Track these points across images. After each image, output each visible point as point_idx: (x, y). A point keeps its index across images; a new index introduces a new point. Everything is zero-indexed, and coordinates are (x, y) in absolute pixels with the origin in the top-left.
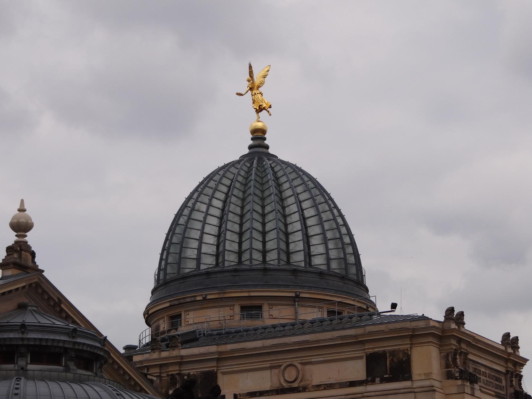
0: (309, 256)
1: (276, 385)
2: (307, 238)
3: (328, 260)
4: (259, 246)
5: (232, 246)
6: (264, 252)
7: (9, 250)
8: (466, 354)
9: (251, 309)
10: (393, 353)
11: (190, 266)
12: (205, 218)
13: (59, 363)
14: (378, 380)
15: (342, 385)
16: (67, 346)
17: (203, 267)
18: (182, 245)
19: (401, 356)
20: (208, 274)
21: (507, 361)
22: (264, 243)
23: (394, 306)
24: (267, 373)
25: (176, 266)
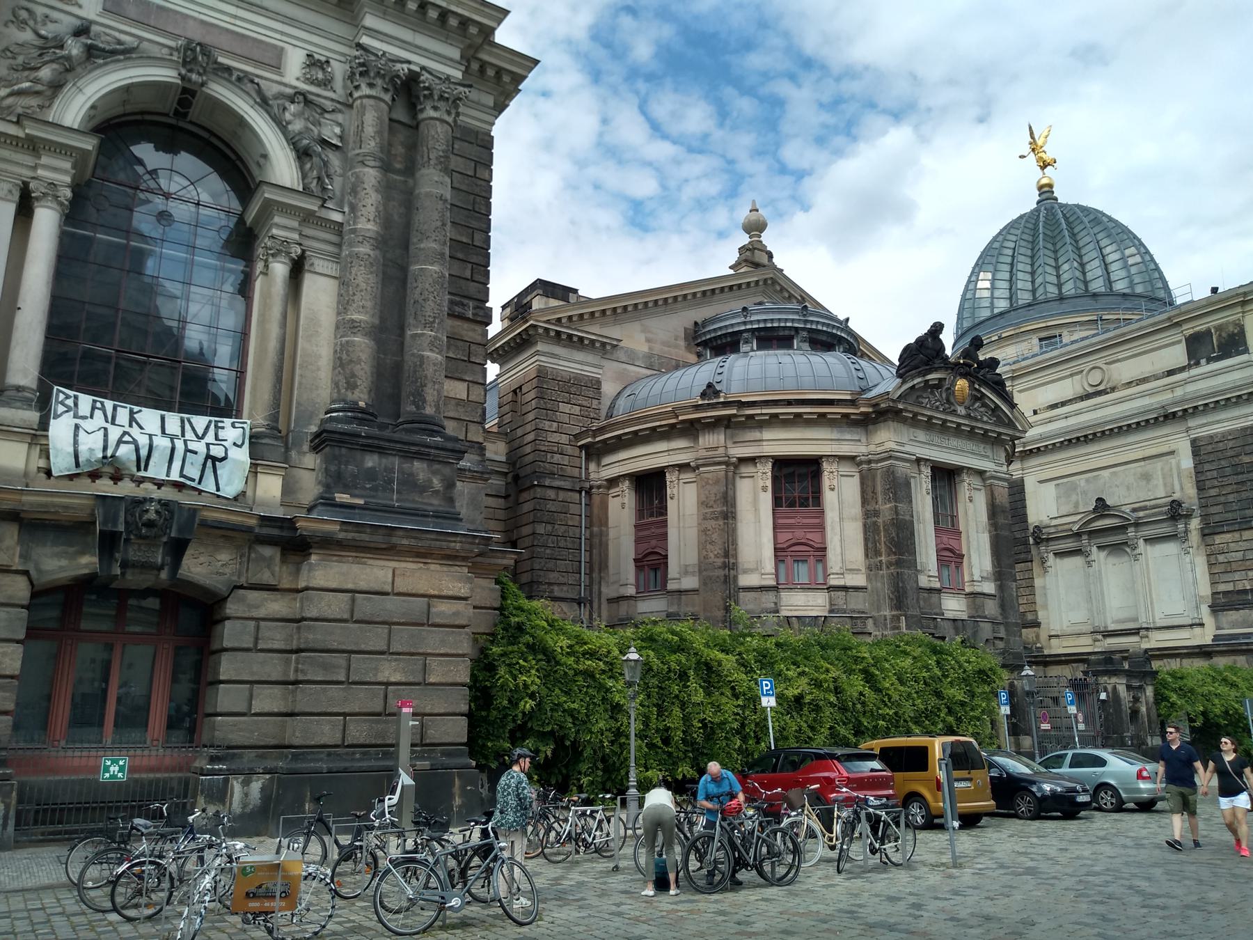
0: (1110, 282)
1: (1079, 391)
3: (1132, 285)
4: (1054, 279)
5: (1023, 282)
6: (1059, 286)
9: (1048, 340)
10: (1219, 328)
13: (790, 347)
14: (1203, 361)
16: (796, 325)
17: (996, 311)
19: (1231, 329)
20: (1001, 314)
22: (1058, 276)
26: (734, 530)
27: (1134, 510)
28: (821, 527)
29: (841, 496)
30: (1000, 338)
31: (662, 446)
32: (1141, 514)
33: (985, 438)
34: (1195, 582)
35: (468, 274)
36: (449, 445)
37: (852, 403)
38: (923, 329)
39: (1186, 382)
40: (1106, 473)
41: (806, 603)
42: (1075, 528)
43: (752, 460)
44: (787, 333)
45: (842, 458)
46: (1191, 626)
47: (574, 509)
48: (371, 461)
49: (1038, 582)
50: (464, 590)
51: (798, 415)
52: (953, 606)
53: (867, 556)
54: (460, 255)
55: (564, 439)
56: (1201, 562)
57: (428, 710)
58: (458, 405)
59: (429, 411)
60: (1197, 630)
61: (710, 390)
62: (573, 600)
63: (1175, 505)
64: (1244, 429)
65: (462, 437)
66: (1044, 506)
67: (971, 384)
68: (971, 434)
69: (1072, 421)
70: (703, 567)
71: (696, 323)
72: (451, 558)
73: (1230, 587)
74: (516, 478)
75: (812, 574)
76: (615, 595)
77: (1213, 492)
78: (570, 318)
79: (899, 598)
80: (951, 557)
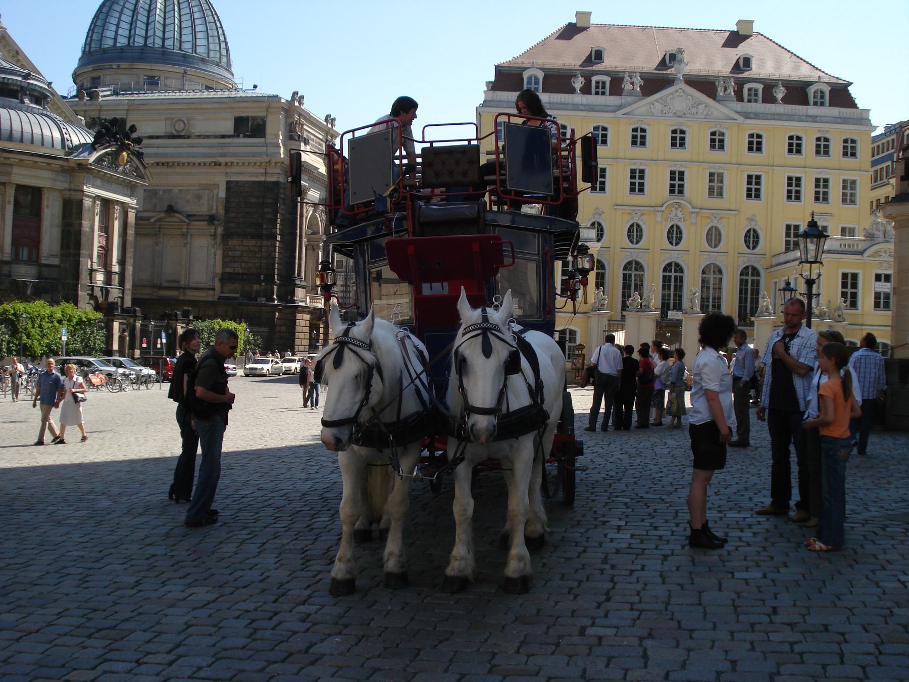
0: (195, 46)
2: (194, 33)
3: (209, 50)
4: (161, 35)
6: (164, 39)
8: (303, 125)
10: (254, 118)
11: (109, 43)
12: (122, 10)
15: (216, 137)
17: (118, 45)
18: (104, 27)
20: (122, 49)
23: (255, 87)
25: (98, 43)
28: (38, 228)
29: (51, 211)
30: (119, 67)
34: (214, 265)
39: (230, 145)
44: (15, 88)
46: (209, 289)
53: (62, 248)
56: (219, 253)
60: (211, 292)
64: (254, 182)
67: (128, 156)
73: (231, 270)
77: (233, 215)
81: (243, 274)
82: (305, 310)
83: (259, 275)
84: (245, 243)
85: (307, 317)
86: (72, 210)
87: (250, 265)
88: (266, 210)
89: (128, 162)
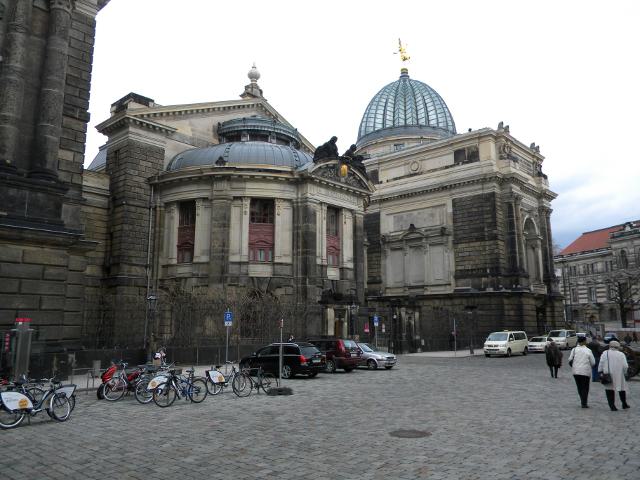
0: (428, 120)
1: (408, 173)
4: (403, 116)
6: (405, 120)
7: (247, 87)
10: (469, 148)
15: (442, 169)
20: (378, 131)
21: (533, 156)
24: (402, 168)
26: (228, 233)
27: (426, 231)
28: (273, 234)
29: (283, 217)
31: (194, 187)
32: (429, 232)
33: (354, 194)
35: (77, 94)
36: (59, 185)
37: (291, 173)
38: (328, 140)
40: (415, 213)
41: (262, 271)
42: (400, 237)
43: (240, 198)
45: (284, 200)
47: (146, 217)
48: (12, 192)
49: (382, 263)
50: (62, 262)
51: (264, 177)
52: (333, 274)
54: (74, 84)
55: (142, 180)
56: (452, 256)
57: (40, 322)
58: (67, 164)
59: (48, 167)
60: (448, 287)
61: (221, 161)
62: (142, 266)
63: (444, 229)
65: (69, 181)
66: (388, 226)
67: (349, 168)
68: (347, 192)
69: (403, 187)
70: (210, 252)
71: (219, 124)
72: (56, 245)
74: (114, 199)
75: (266, 257)
76: (165, 264)
78: (148, 115)
79: (306, 270)
80: (335, 250)
81: (472, 270)
82: (531, 295)
83: (485, 269)
84: (472, 244)
85: (533, 302)
86: (302, 214)
87: (477, 261)
88: (486, 216)
89: (350, 175)
